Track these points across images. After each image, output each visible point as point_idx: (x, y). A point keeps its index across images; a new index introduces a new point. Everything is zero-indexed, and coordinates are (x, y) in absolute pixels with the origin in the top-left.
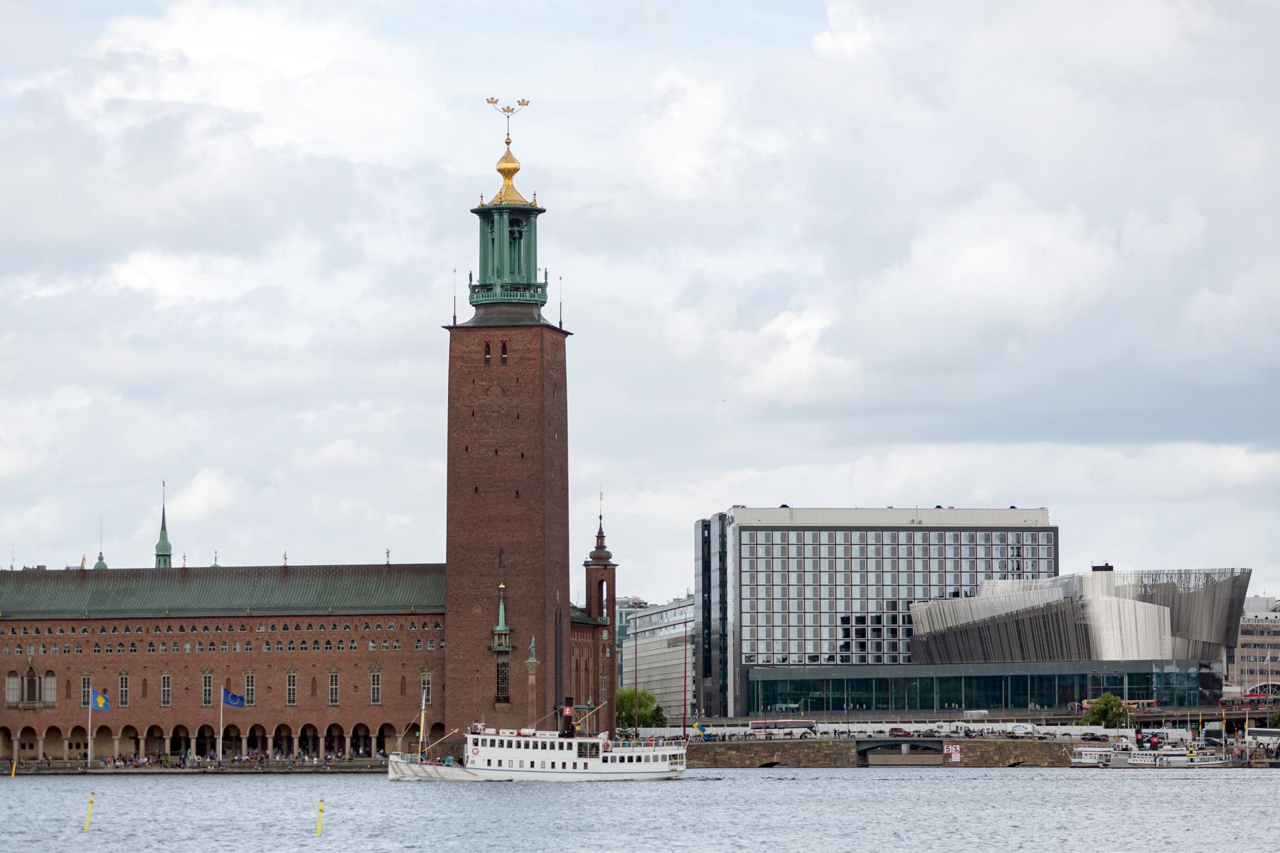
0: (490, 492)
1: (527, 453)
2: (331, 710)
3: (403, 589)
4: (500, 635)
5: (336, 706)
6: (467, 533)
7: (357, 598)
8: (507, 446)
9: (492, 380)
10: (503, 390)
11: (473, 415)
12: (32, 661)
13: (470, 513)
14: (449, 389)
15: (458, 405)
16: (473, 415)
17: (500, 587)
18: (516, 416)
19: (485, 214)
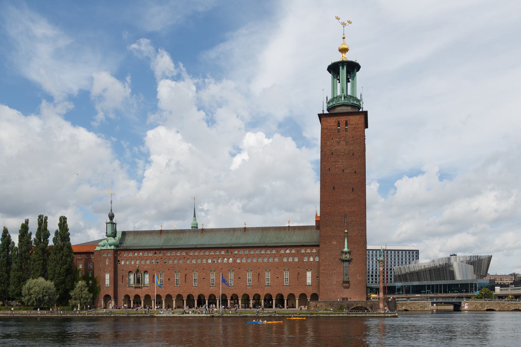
0: (340, 189)
1: (357, 170)
2: (267, 287)
3: (296, 236)
4: (346, 253)
5: (269, 286)
6: (330, 208)
7: (277, 240)
8: (348, 168)
9: (341, 138)
10: (346, 142)
11: (332, 154)
12: (138, 267)
13: (331, 198)
14: (321, 143)
15: (325, 150)
16: (332, 154)
17: (345, 231)
18: (352, 154)
19: (334, 69)
